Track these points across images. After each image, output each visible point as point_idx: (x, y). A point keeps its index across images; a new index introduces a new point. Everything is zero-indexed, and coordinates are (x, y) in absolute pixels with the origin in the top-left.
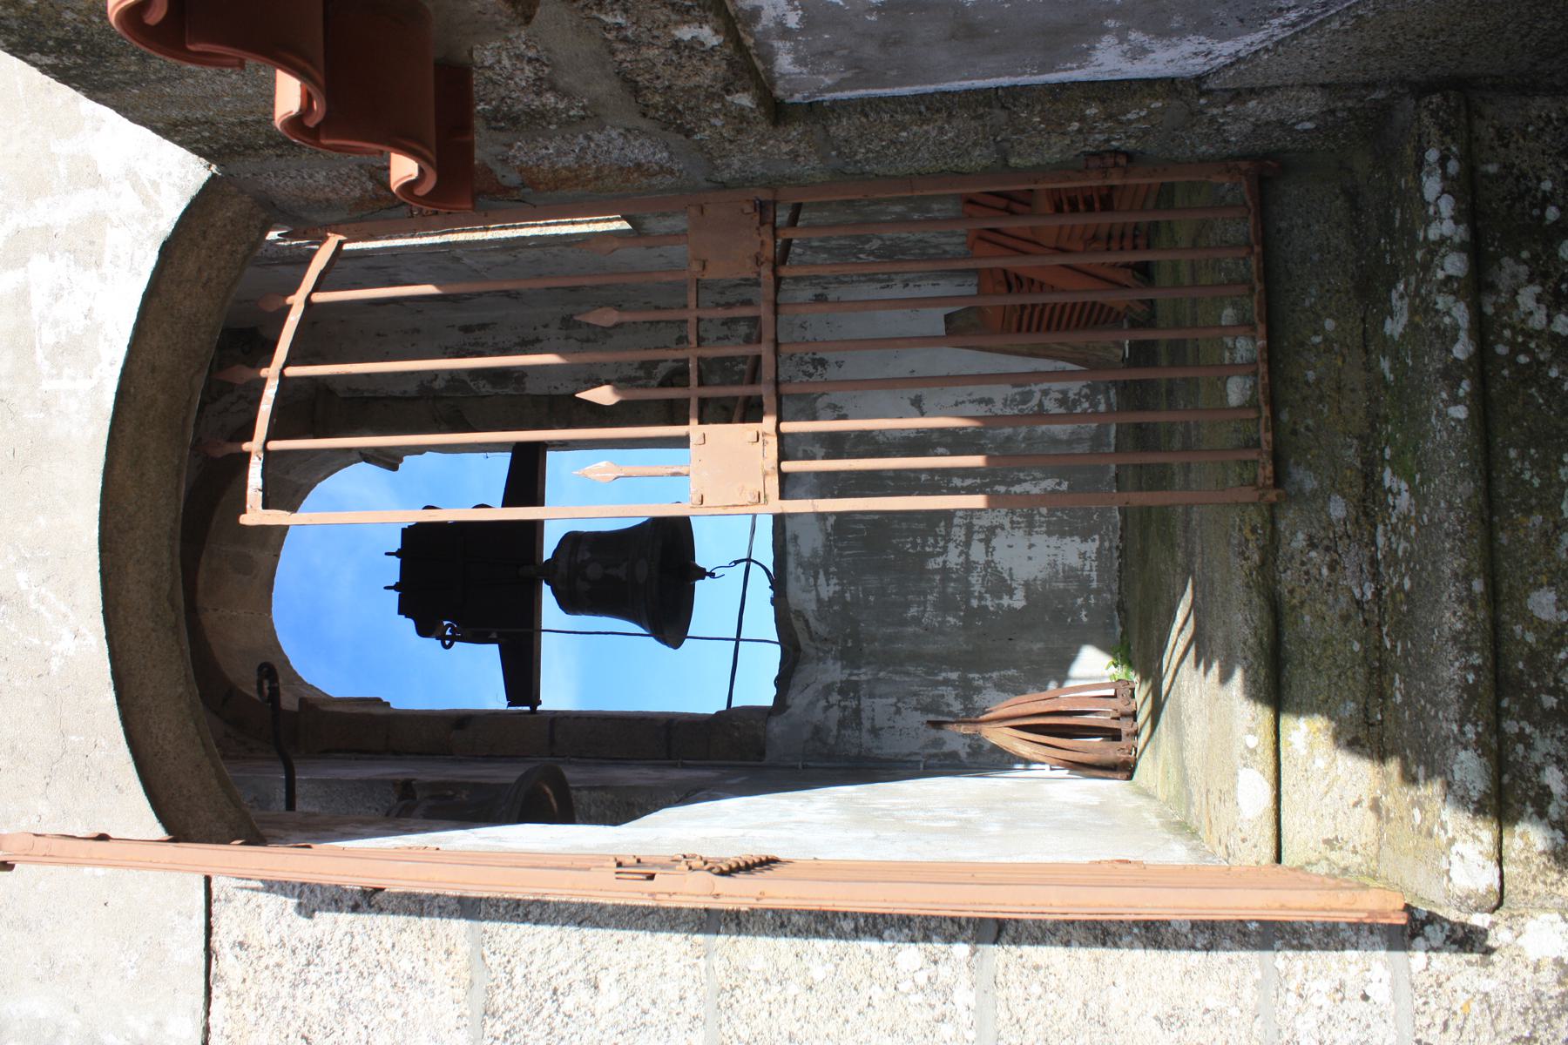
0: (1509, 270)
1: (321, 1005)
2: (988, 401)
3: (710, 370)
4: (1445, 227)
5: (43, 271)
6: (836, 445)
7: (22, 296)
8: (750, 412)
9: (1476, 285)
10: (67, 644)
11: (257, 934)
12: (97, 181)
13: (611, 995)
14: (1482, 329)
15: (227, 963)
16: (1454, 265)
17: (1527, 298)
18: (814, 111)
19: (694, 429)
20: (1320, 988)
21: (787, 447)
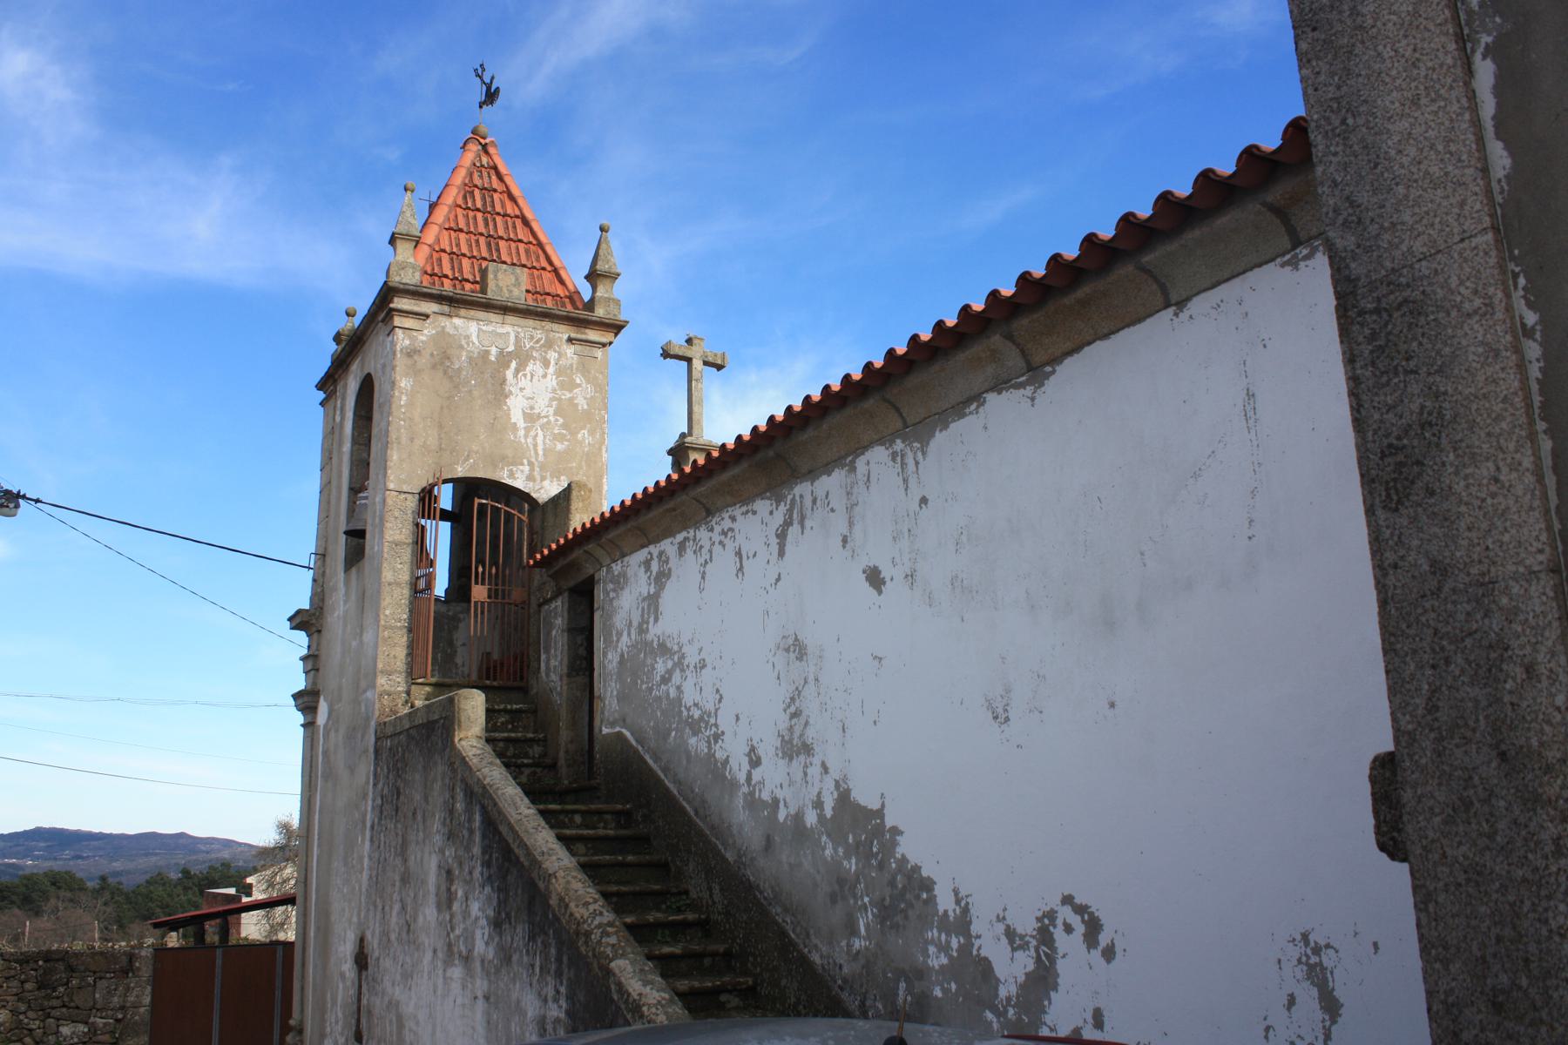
0: (507, 717)
1: (397, 514)
2: (463, 665)
3: (496, 590)
4: (515, 706)
5: (526, 469)
6: (482, 613)
7: (522, 464)
8: (489, 597)
9: (506, 711)
10: (460, 469)
11: (408, 503)
12: (541, 481)
13: (399, 566)
14: (499, 711)
15: (403, 496)
16: (509, 707)
17: (503, 719)
18: (540, 611)
19: (487, 587)
20: (399, 680)
21: (483, 603)
